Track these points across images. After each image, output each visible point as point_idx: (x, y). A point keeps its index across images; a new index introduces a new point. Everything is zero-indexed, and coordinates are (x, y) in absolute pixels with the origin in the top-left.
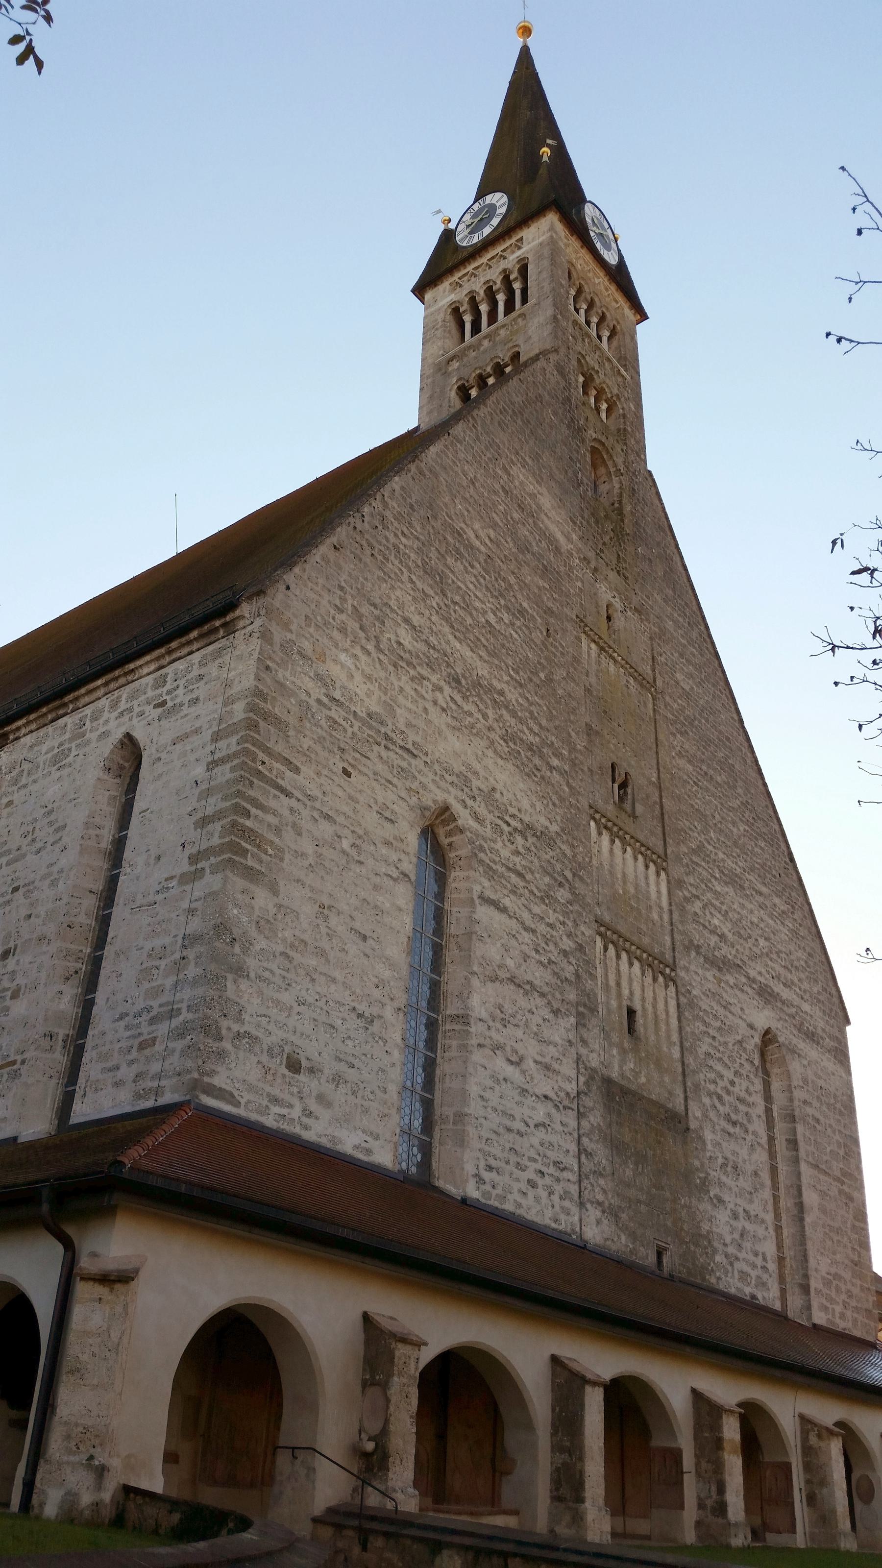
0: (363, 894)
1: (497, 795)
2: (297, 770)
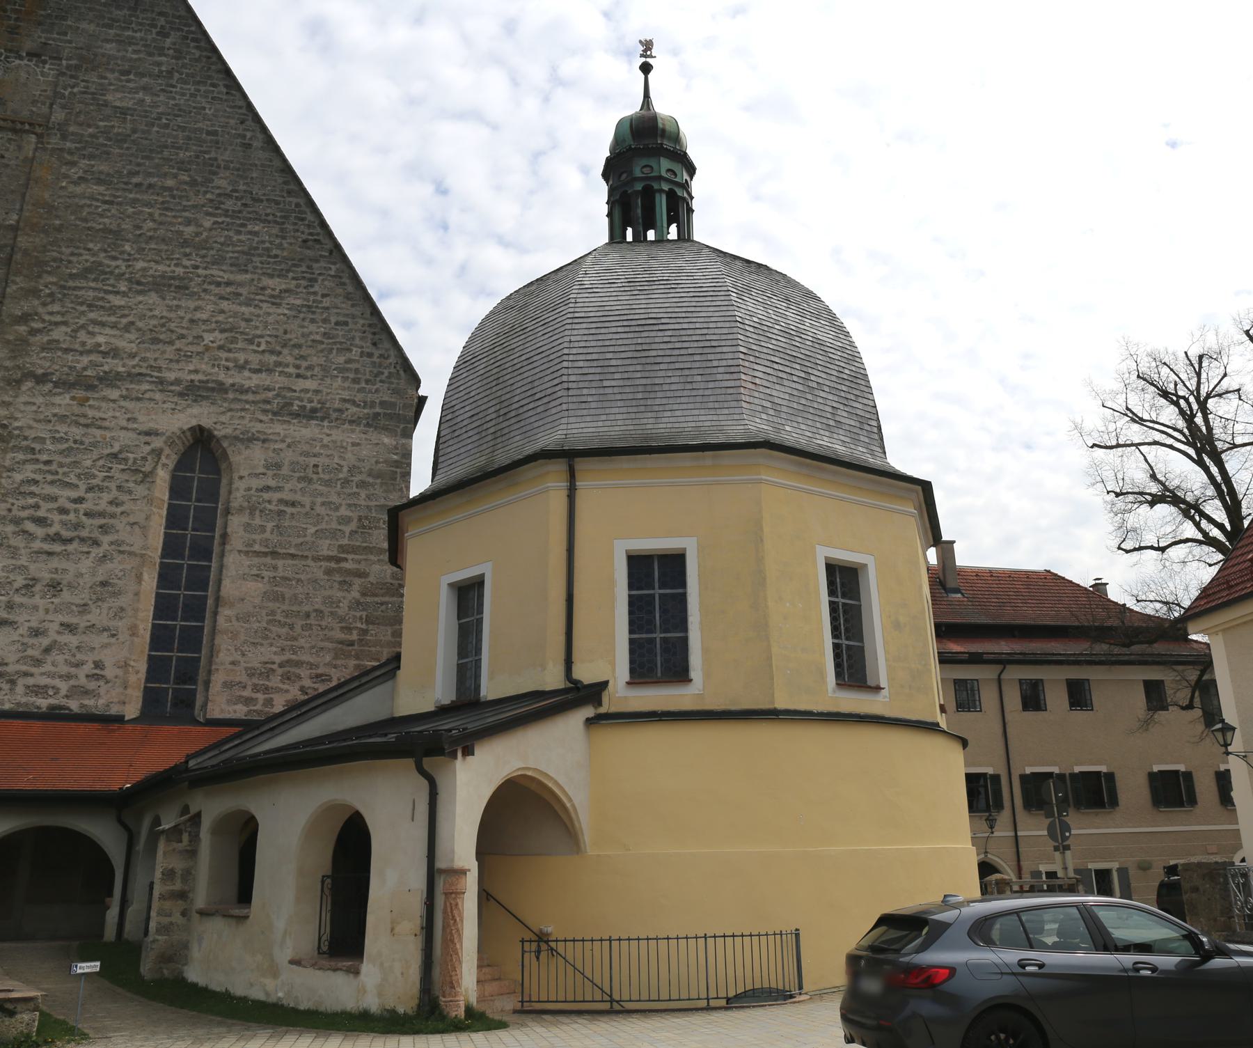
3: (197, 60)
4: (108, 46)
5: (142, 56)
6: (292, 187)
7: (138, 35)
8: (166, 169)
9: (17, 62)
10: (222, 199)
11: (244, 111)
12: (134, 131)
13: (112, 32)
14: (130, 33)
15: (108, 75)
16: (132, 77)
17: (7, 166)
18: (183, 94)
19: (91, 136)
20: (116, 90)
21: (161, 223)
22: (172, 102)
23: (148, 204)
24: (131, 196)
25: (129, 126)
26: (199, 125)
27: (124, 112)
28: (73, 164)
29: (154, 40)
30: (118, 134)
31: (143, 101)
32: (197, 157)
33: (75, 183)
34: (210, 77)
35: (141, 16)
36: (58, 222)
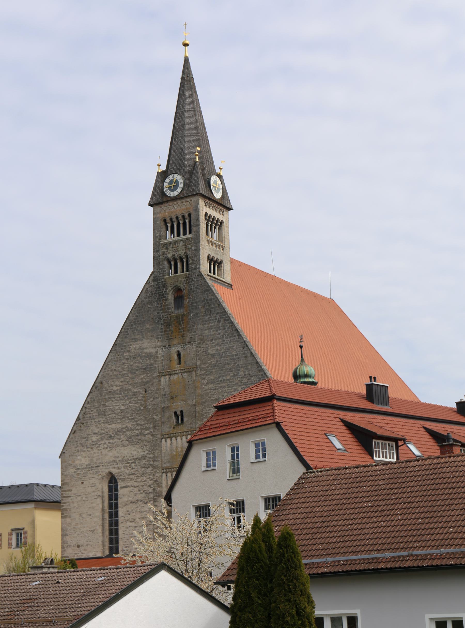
0: (89, 506)
1: (126, 458)
2: (71, 490)
3: (229, 328)
4: (206, 332)
5: (215, 332)
6: (260, 368)
7: (213, 324)
8: (227, 373)
9: (186, 346)
10: (242, 379)
11: (243, 344)
12: (217, 361)
13: (206, 326)
14: (211, 325)
15: (208, 343)
16: (214, 341)
17: (190, 384)
18: (227, 343)
19: (208, 367)
20: (211, 348)
21: (228, 393)
22: (225, 347)
23: (224, 387)
24: (220, 385)
25: (216, 360)
26: (233, 353)
27: (213, 355)
28: (204, 379)
29: (217, 324)
30: (214, 364)
31: (217, 349)
32: (234, 365)
33: (206, 385)
34: (233, 333)
35: (213, 316)
36: (204, 400)
